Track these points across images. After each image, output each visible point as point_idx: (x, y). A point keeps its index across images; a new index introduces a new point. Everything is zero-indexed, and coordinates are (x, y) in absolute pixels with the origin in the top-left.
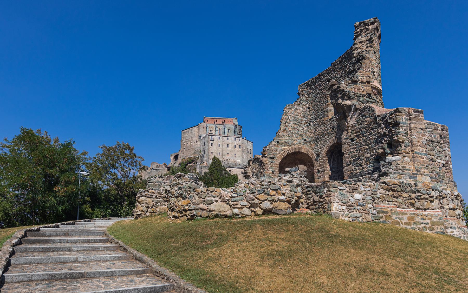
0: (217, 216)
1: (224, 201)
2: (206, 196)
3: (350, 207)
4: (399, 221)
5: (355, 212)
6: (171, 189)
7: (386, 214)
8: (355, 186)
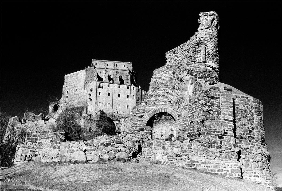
7: (197, 163)
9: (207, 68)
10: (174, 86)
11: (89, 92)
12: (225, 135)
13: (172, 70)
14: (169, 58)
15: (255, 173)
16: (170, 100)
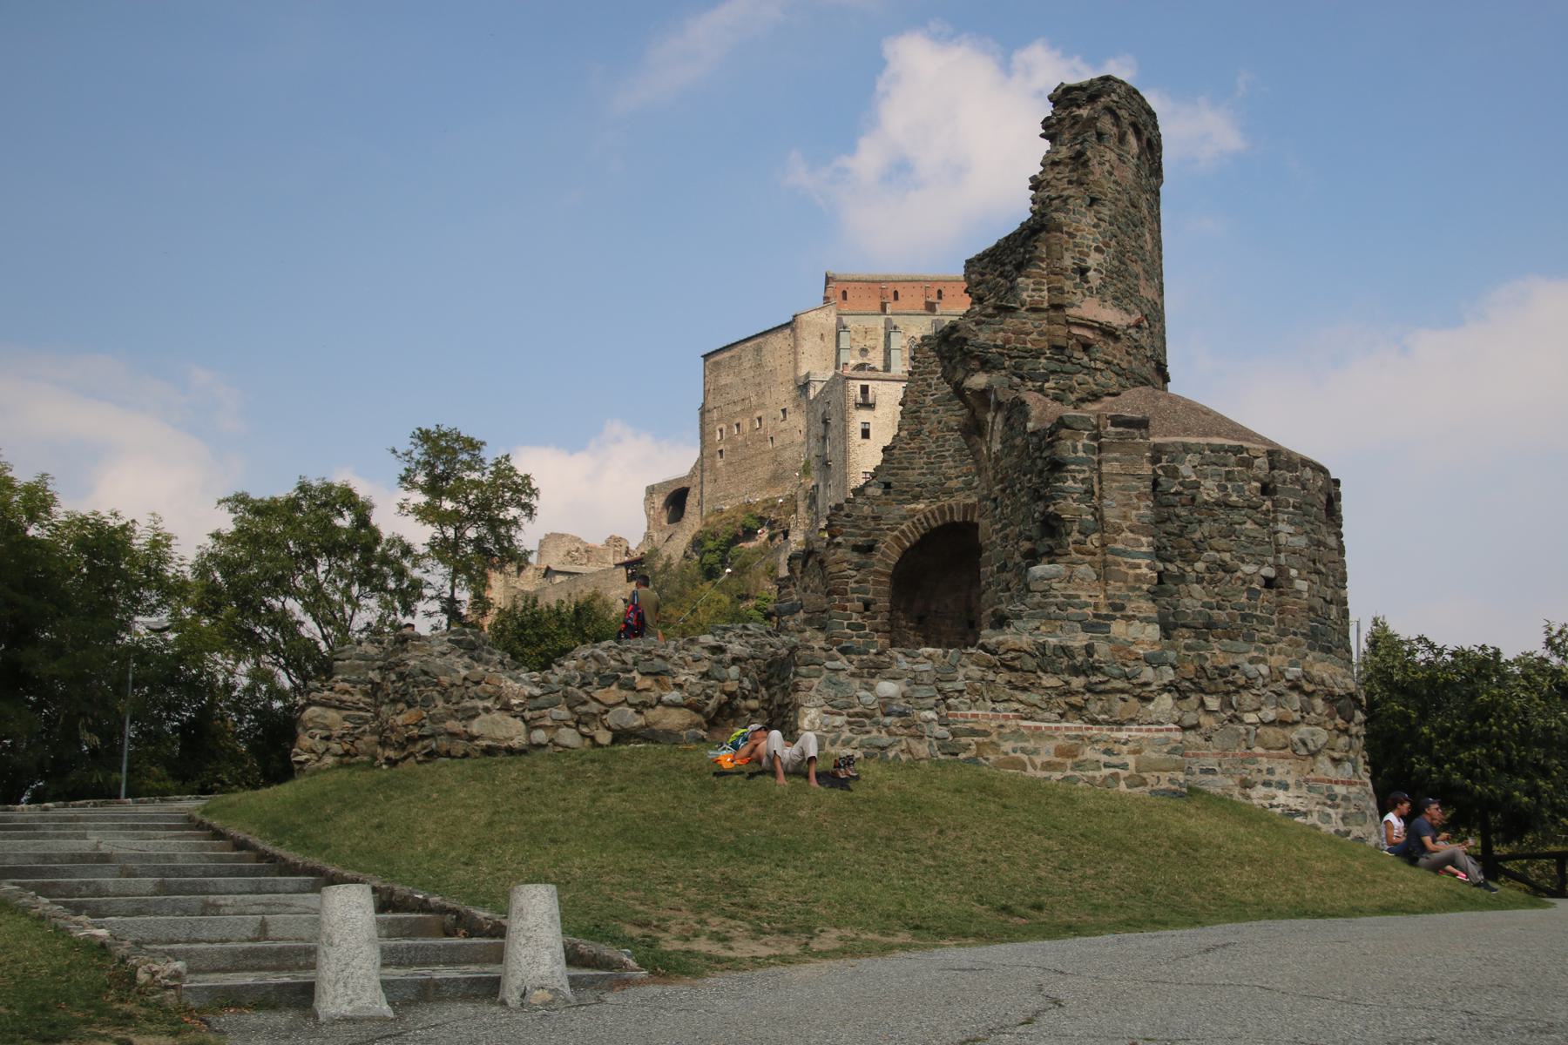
0: (489, 751)
1: (507, 708)
3: (860, 719)
4: (1024, 757)
5: (875, 733)
6: (383, 679)
8: (882, 658)
9: (1076, 331)
12: (1114, 618)
14: (979, 284)
15: (1270, 771)
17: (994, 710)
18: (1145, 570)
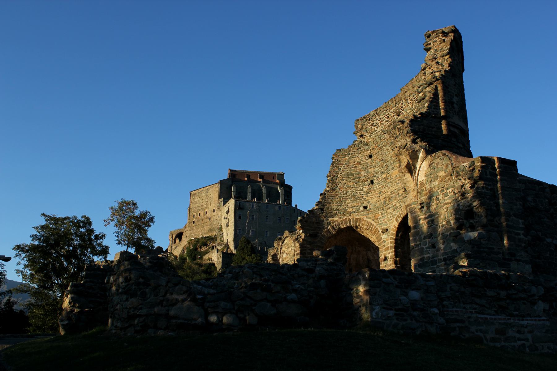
2: (166, 293)
4: (482, 335)
10: (372, 179)
11: (226, 215)
13: (368, 150)
14: (362, 128)
16: (365, 204)
17: (464, 308)
18: (522, 236)
